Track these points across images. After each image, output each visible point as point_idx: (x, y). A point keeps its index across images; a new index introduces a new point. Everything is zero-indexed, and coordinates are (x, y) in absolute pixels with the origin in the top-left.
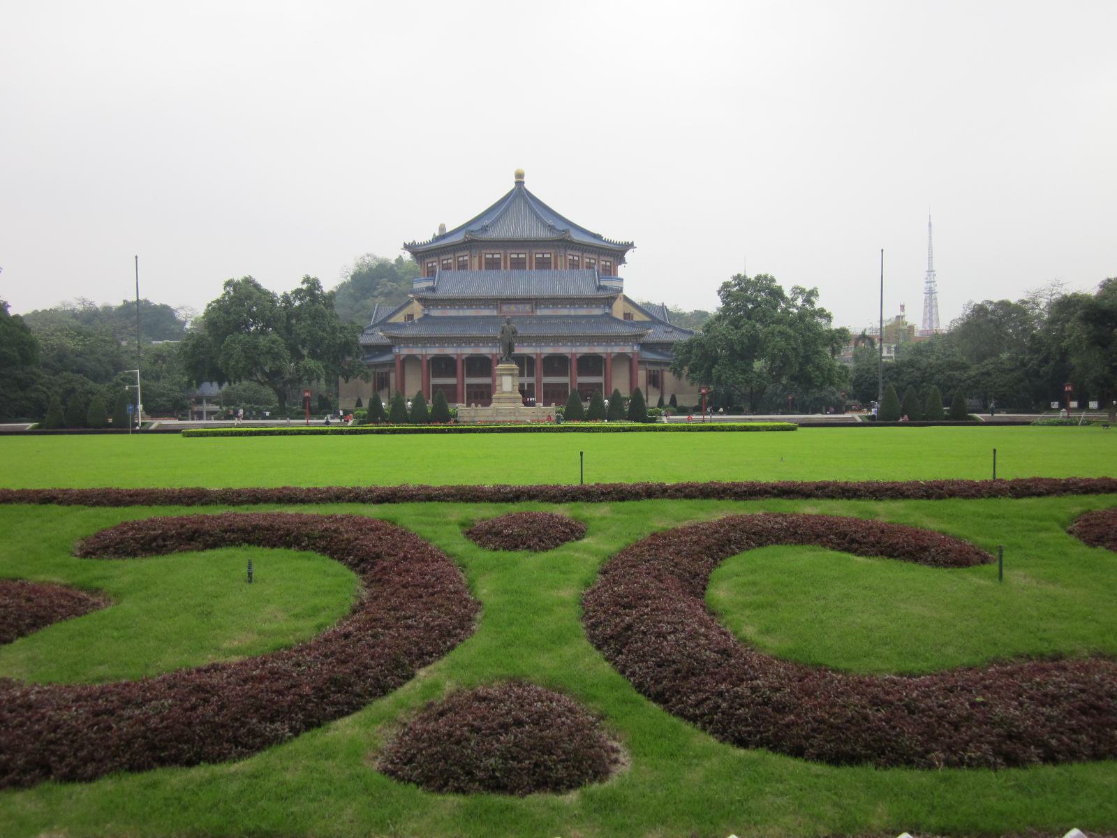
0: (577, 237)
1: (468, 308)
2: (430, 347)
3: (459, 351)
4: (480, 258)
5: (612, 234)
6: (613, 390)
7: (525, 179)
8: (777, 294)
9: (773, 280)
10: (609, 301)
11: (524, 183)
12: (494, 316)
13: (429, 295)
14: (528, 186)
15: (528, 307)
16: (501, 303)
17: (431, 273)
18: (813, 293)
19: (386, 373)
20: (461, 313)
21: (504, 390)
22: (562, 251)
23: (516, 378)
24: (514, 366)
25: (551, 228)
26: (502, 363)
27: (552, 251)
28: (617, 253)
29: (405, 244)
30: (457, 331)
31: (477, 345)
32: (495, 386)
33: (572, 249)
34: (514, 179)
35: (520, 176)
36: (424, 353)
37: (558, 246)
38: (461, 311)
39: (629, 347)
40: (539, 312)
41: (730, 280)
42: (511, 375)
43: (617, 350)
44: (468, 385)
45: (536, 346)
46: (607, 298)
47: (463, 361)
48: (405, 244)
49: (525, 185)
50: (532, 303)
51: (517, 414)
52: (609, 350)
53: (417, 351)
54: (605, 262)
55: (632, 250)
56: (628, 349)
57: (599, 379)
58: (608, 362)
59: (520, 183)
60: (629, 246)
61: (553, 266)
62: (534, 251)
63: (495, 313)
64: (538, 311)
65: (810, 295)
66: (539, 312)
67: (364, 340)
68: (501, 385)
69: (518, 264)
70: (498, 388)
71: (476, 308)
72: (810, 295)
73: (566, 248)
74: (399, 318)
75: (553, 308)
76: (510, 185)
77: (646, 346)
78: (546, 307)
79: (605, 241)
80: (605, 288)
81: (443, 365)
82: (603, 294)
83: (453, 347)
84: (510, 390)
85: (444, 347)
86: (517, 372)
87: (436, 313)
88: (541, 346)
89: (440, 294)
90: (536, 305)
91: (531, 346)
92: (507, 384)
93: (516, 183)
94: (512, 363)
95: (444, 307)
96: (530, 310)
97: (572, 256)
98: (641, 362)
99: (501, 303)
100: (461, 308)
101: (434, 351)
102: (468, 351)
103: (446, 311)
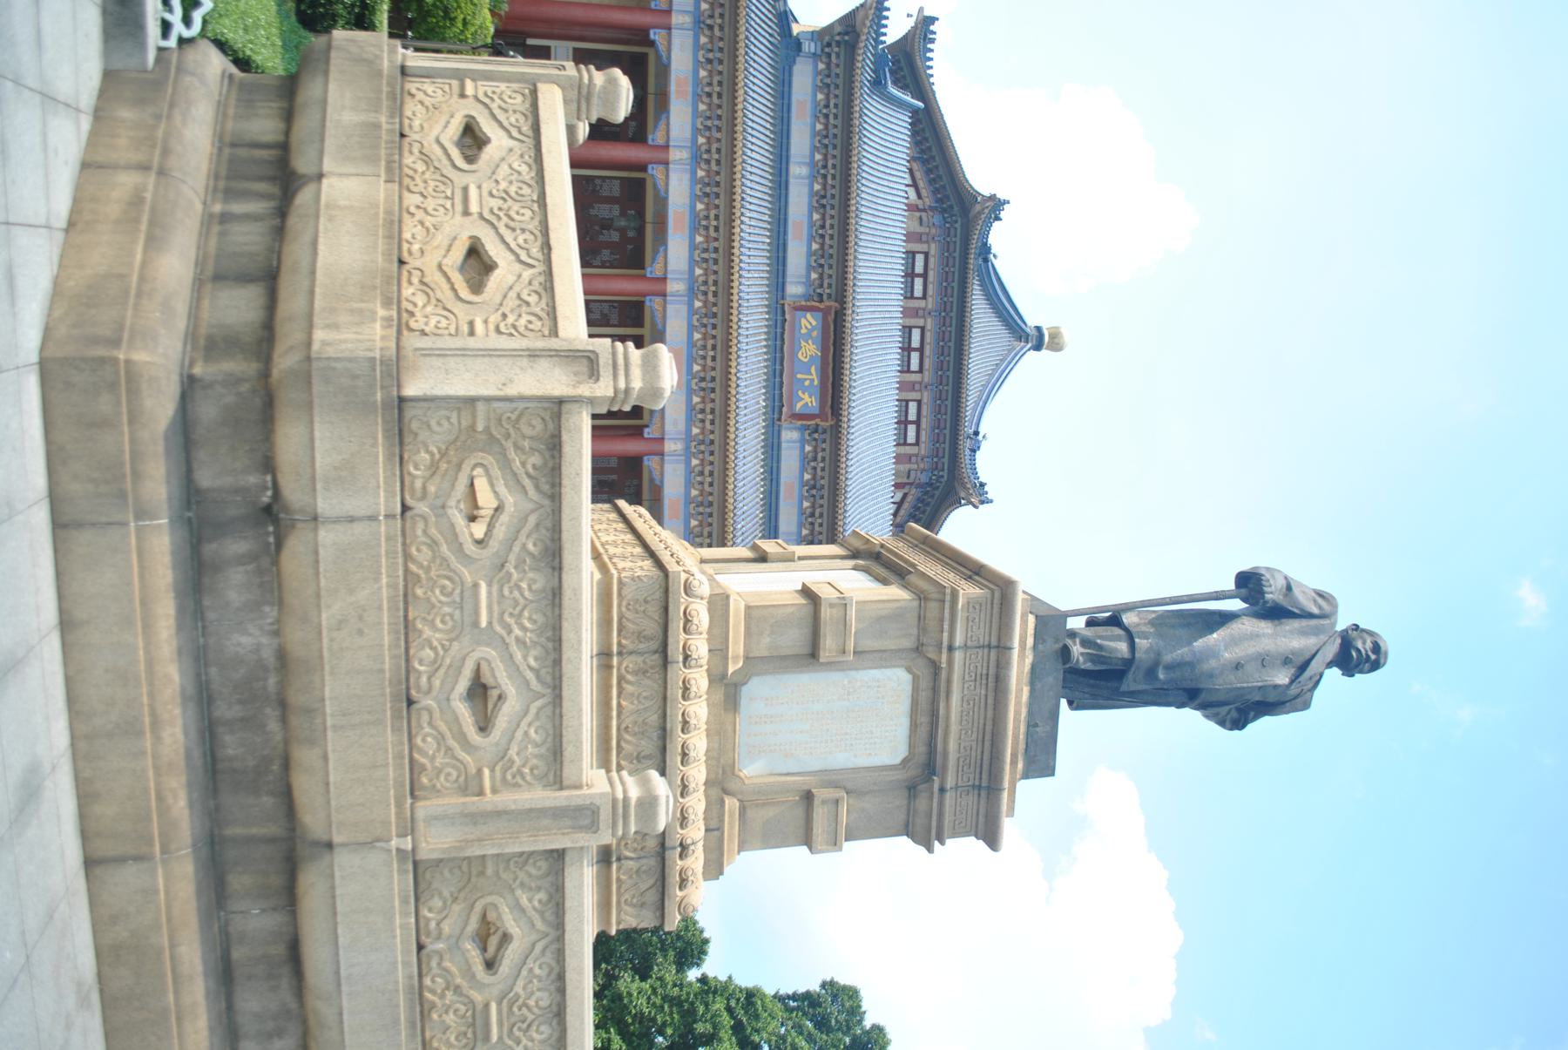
1: (812, 194)
2: (697, 47)
3: (678, 155)
7: (1044, 352)
15: (807, 401)
22: (924, 478)
29: (932, 20)
31: (697, 223)
33: (920, 500)
34: (1045, 326)
38: (804, 171)
45: (689, 438)
47: (643, 168)
48: (932, 20)
50: (821, 415)
59: (1038, 340)
63: (794, 289)
64: (795, 435)
66: (790, 436)
71: (811, 224)
75: (803, 484)
76: (1032, 317)
78: (806, 461)
83: (696, 132)
85: (697, 98)
87: (803, 78)
88: (688, 455)
91: (690, 421)
95: (821, 113)
96: (798, 407)
99: (826, 312)
100: (818, 172)
103: (809, 120)
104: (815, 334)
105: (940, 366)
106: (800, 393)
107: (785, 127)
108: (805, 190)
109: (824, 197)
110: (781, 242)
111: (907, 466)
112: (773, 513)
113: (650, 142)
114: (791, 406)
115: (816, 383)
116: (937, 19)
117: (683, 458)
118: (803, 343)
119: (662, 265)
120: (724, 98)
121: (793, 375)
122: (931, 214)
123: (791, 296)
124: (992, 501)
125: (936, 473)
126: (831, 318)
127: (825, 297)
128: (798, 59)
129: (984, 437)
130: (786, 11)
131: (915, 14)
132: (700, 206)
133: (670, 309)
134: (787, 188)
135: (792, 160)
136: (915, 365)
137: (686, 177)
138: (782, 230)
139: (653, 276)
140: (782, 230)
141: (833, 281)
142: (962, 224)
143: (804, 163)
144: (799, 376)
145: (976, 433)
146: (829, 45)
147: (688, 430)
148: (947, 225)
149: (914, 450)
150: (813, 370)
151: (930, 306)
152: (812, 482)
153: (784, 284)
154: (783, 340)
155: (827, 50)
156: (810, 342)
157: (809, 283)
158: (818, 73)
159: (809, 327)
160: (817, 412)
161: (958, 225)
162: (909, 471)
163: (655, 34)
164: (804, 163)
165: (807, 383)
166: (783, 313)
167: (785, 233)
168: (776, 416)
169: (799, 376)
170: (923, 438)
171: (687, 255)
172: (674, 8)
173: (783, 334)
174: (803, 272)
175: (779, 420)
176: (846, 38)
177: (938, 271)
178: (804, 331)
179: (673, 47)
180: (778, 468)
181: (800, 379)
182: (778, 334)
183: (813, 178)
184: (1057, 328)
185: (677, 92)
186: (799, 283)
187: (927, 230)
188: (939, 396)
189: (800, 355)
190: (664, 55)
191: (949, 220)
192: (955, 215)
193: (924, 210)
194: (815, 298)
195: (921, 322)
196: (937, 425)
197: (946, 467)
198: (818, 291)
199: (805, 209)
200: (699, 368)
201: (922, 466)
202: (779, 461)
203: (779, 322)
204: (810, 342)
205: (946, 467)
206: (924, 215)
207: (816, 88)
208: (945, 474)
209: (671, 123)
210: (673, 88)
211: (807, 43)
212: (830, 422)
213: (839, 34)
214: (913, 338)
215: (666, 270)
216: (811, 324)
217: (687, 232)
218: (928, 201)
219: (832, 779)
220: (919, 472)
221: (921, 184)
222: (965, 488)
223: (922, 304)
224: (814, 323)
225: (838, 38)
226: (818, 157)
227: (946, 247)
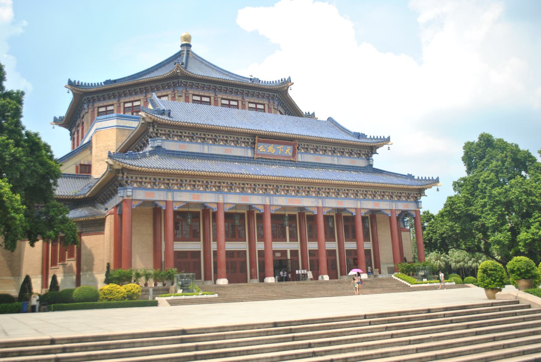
1: (214, 144)
2: (179, 190)
7: (192, 43)
12: (250, 158)
15: (288, 150)
36: (170, 199)
37: (273, 98)
38: (206, 147)
63: (249, 153)
64: (299, 156)
66: (300, 158)
90: (298, 148)
96: (290, 154)
99: (259, 141)
103: (186, 144)
104: (265, 146)
105: (236, 93)
106: (286, 153)
107: (190, 154)
108: (213, 147)
109: (215, 140)
110: (233, 158)
111: (273, 109)
112: (325, 165)
113: (216, 210)
114: (289, 157)
115: (282, 147)
116: (69, 79)
117: (324, 199)
118: (269, 151)
119: (259, 206)
120: (199, 179)
121: (279, 156)
122: (176, 91)
123: (252, 155)
124: (290, 77)
125: (275, 98)
127: (253, 141)
128: (163, 147)
129: (251, 76)
130: (149, 152)
131: (68, 89)
132: (238, 191)
133: (275, 203)
134: (213, 154)
135: (202, 152)
136: (235, 103)
137: (229, 196)
138: (228, 157)
139: (263, 210)
140: (228, 157)
141: (246, 138)
142: (182, 79)
143: (203, 147)
144: (280, 153)
145: (251, 79)
146: (157, 134)
148: (182, 85)
150: (278, 148)
151: (213, 95)
152: (314, 150)
153: (248, 157)
154: (268, 159)
155: (159, 135)
156: (268, 148)
158: (167, 139)
159: (263, 148)
160: (292, 147)
161: (183, 81)
162: (274, 109)
163: (175, 208)
164: (203, 147)
165: (282, 150)
166: (259, 158)
167: (230, 156)
168: (294, 163)
169: (280, 153)
171: (256, 196)
172: (165, 200)
173: (266, 159)
175: (295, 162)
176: (156, 126)
177: (200, 90)
178: (264, 150)
179: (181, 200)
180: (311, 163)
181: (281, 153)
182: (266, 161)
183: (208, 144)
184: (181, 37)
185: (198, 199)
186: (247, 151)
187: (184, 94)
189: (272, 152)
190: (183, 204)
191: (180, 84)
192: (178, 81)
193: (175, 94)
194: (252, 145)
197: (273, 94)
198: (250, 144)
200: (293, 193)
201: (272, 103)
202: (308, 162)
203: (261, 160)
204: (268, 148)
205: (273, 94)
206: (176, 94)
208: (275, 94)
209: (209, 201)
210: (196, 201)
211: (158, 143)
212: (297, 142)
213: (153, 129)
214: (225, 103)
215: (261, 205)
216: (262, 147)
217: (248, 196)
218: (169, 92)
220: (275, 105)
222: (283, 87)
224: (262, 146)
225: (155, 130)
227: (191, 87)
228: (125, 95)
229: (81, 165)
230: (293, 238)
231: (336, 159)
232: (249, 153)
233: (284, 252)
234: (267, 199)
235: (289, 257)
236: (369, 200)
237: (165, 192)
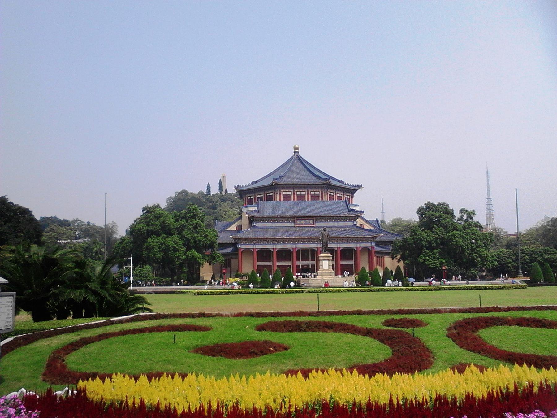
0: (334, 183)
4: (280, 194)
5: (350, 181)
6: (361, 267)
8: (450, 213)
9: (448, 205)
10: (356, 217)
11: (298, 152)
13: (256, 215)
14: (300, 154)
15: (311, 222)
16: (296, 219)
17: (250, 202)
18: (473, 213)
19: (229, 259)
20: (274, 225)
21: (324, 268)
22: (326, 190)
23: (331, 261)
24: (329, 255)
25: (319, 177)
26: (323, 253)
27: (320, 190)
28: (352, 190)
30: (273, 235)
32: (319, 266)
35: (295, 148)
38: (274, 224)
39: (370, 244)
40: (317, 224)
41: (423, 205)
42: (328, 260)
43: (363, 245)
44: (277, 266)
46: (355, 216)
49: (299, 153)
51: (335, 282)
52: (358, 245)
53: (250, 247)
54: (346, 197)
55: (361, 189)
56: (368, 245)
57: (351, 262)
58: (358, 252)
60: (359, 187)
61: (320, 198)
62: (310, 190)
64: (317, 223)
65: (471, 214)
67: (220, 240)
68: (322, 266)
69: (301, 197)
70: (320, 267)
72: (471, 214)
73: (328, 188)
74: (233, 228)
75: (325, 222)
77: (378, 244)
79: (345, 184)
80: (353, 210)
81: (264, 255)
82: (352, 214)
83: (271, 244)
84: (327, 268)
86: (331, 258)
87: (260, 225)
89: (262, 214)
90: (316, 220)
92: (326, 265)
93: (295, 152)
94: (328, 253)
95: (264, 222)
96: (312, 223)
97: (331, 193)
98: (375, 252)
101: (260, 246)
102: (280, 246)
103: (266, 224)
104: (300, 221)
126: (297, 218)
147: (316, 244)
149: (320, 192)
157: (292, 222)
158: (258, 222)
170: (318, 190)
174: (290, 223)
188: (310, 188)
195: (296, 192)
196: (315, 188)
199: (280, 223)
207: (261, 222)
212: (315, 218)
219: (329, 265)
221: (269, 192)
223: (292, 192)
226: (271, 222)
227: (282, 188)
228: (257, 192)
229: (238, 226)
230: (313, 260)
231: (336, 223)
232: (293, 225)
233: (308, 266)
234: (294, 245)
235: (310, 268)
236: (344, 243)
237: (253, 245)
